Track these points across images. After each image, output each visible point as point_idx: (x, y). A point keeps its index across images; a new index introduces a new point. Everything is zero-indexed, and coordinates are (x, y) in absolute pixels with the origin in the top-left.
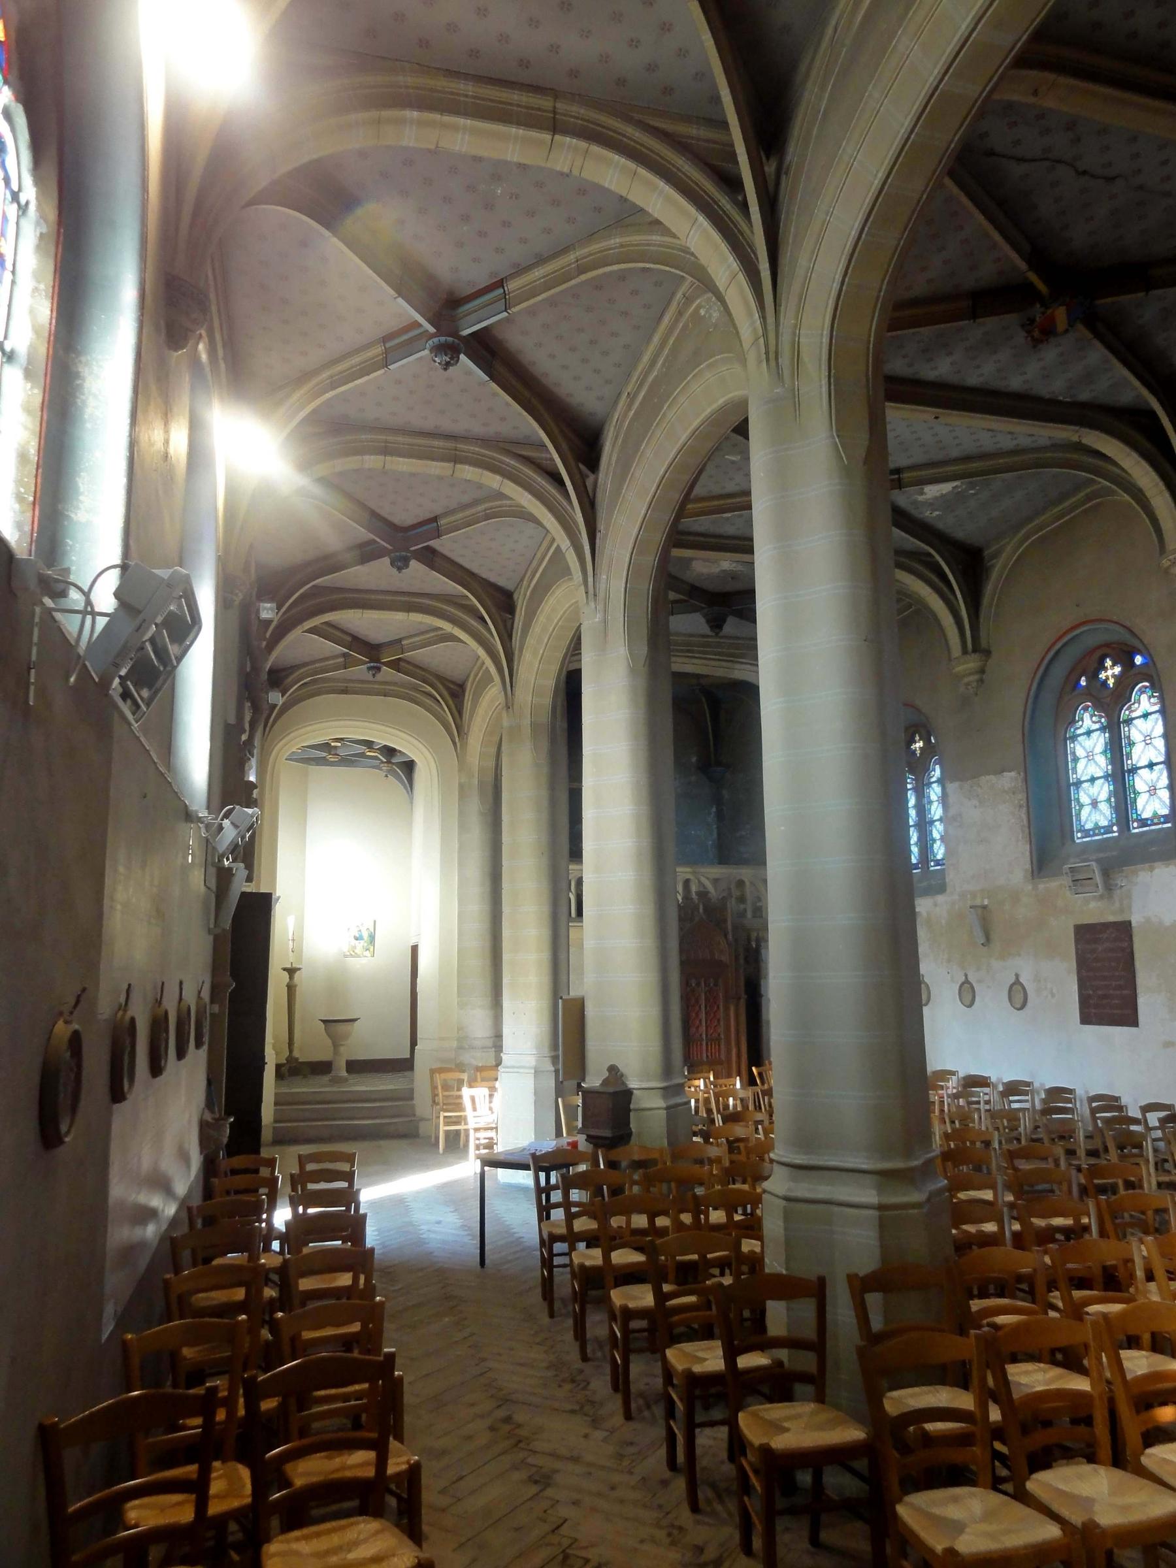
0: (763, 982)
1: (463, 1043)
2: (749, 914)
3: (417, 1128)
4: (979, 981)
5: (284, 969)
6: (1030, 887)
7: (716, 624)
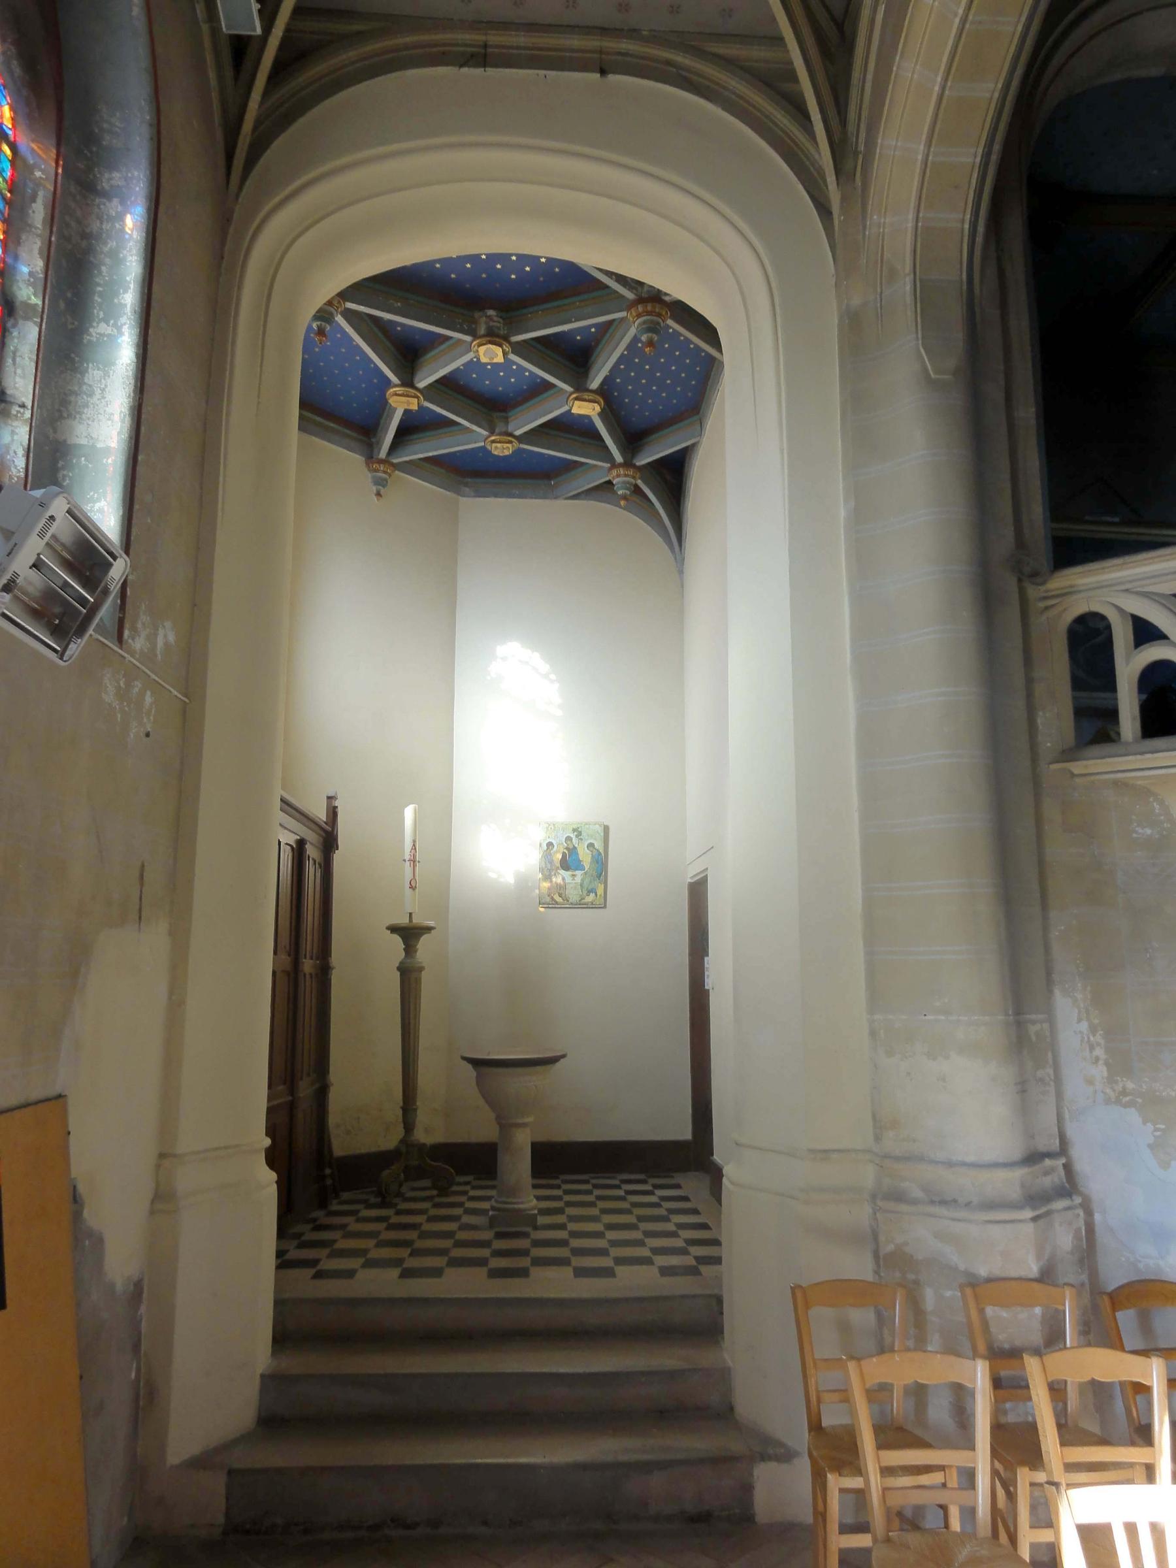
1: (896, 1182)
3: (747, 1489)
5: (394, 929)
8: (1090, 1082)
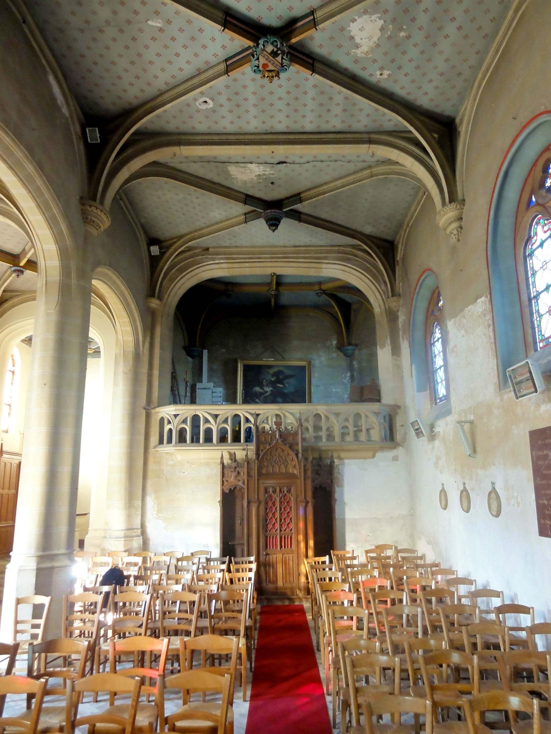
0: (337, 489)
2: (324, 440)
4: (472, 489)
6: (498, 400)
7: (274, 223)
8: (153, 515)
